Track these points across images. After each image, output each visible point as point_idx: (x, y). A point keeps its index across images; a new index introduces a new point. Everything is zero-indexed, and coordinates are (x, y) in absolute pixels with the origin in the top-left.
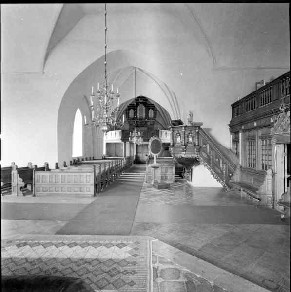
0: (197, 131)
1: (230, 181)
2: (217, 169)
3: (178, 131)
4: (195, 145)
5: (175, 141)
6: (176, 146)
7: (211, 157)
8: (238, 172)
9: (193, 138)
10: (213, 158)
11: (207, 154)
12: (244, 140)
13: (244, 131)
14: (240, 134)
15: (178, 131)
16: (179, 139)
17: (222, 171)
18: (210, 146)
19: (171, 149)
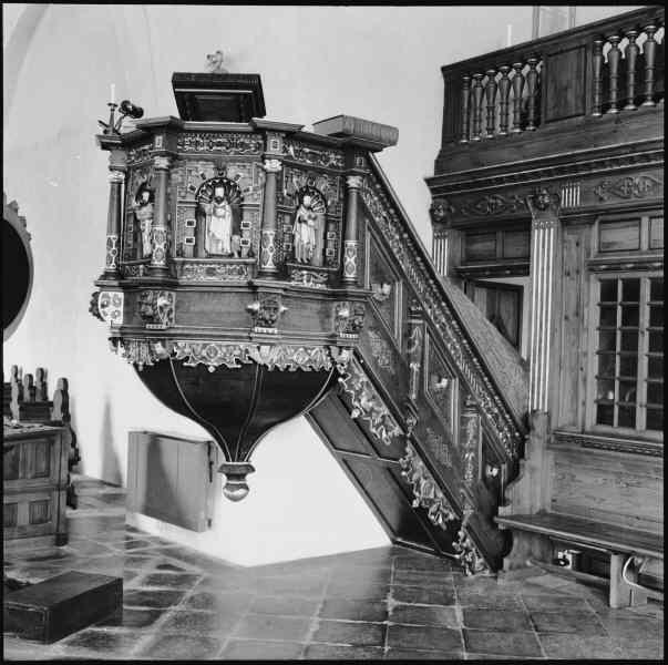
0: (353, 182)
1: (501, 510)
2: (435, 441)
3: (220, 169)
4: (337, 279)
5: (185, 235)
6: (196, 276)
7: (415, 366)
8: (538, 459)
9: (335, 223)
10: (421, 369)
11: (391, 344)
12: (564, 272)
13: (568, 221)
14: (543, 242)
15: (220, 169)
16: (219, 227)
17: (459, 462)
18: (410, 293)
19: (161, 301)
